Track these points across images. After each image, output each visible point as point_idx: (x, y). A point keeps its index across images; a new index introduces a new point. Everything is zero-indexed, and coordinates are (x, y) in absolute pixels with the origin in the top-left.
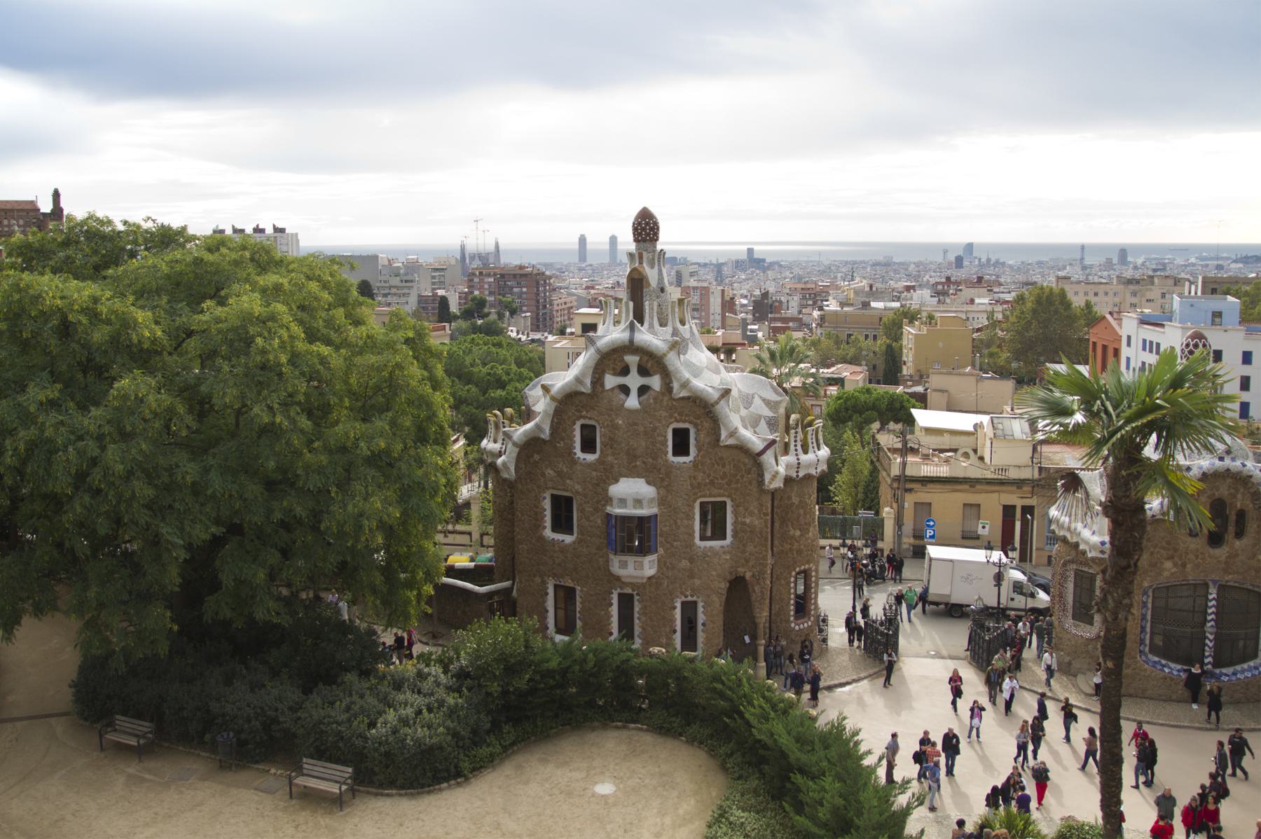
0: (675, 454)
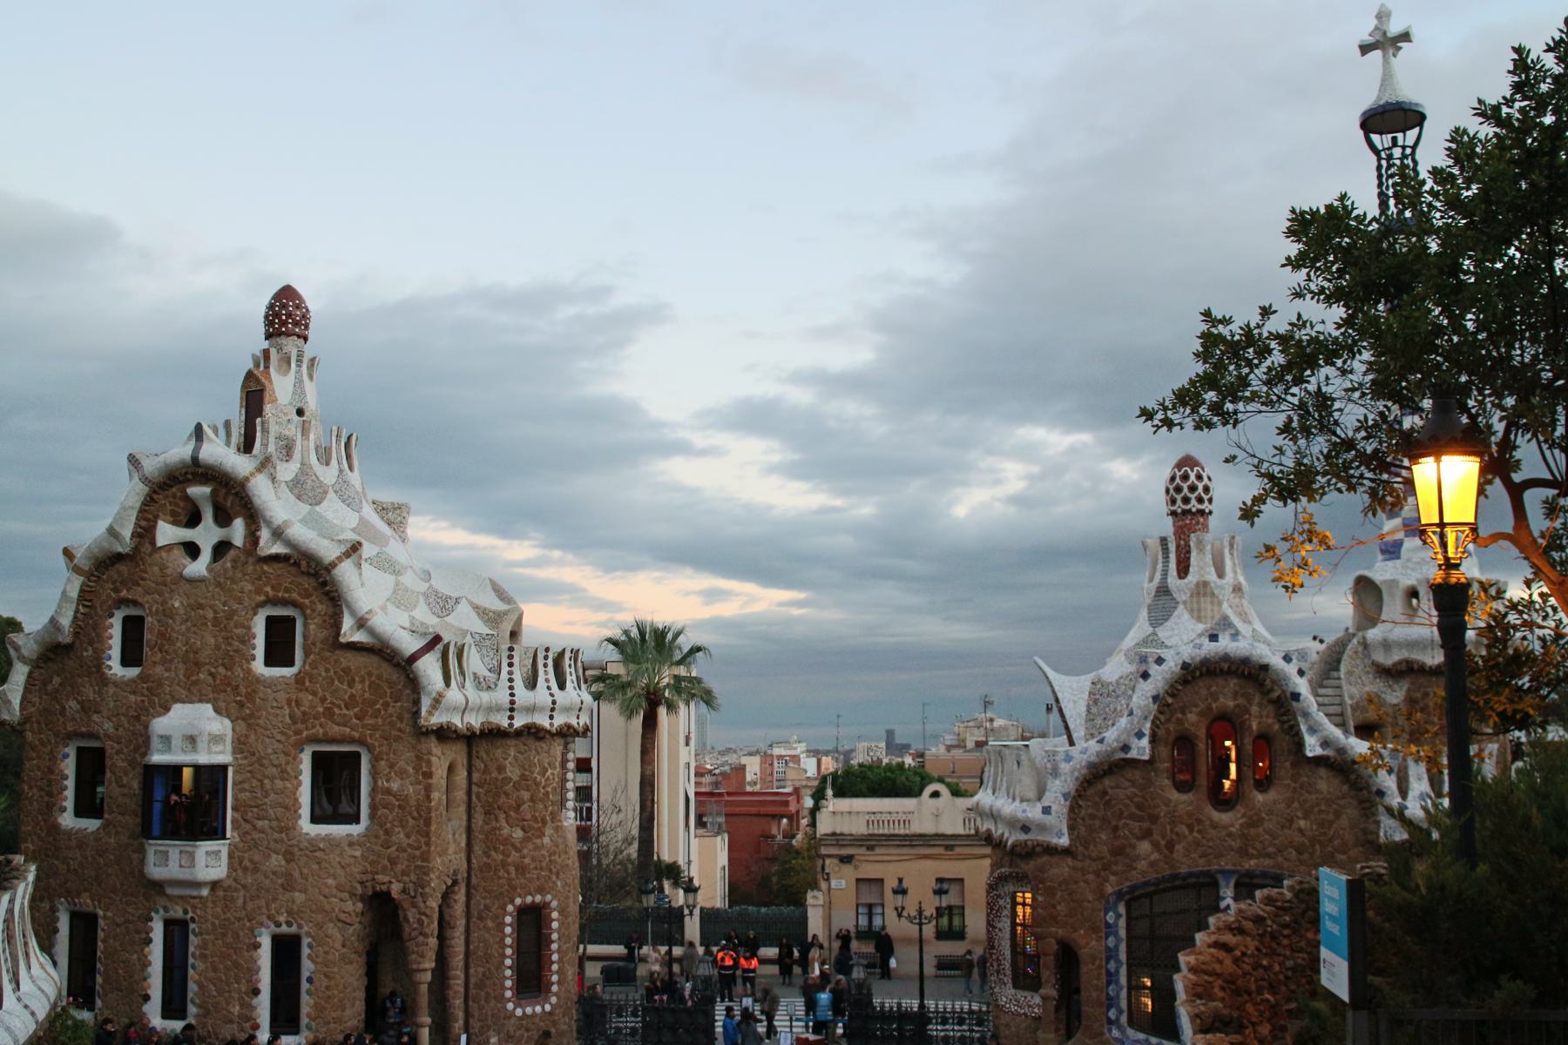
0: (269, 662)
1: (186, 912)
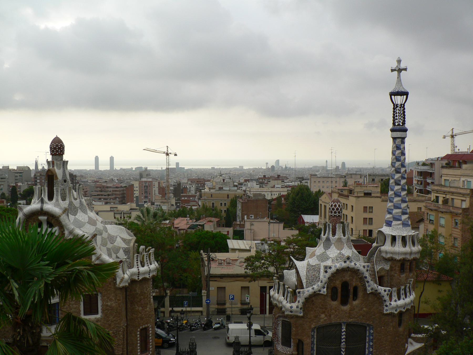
1: (47, 344)
